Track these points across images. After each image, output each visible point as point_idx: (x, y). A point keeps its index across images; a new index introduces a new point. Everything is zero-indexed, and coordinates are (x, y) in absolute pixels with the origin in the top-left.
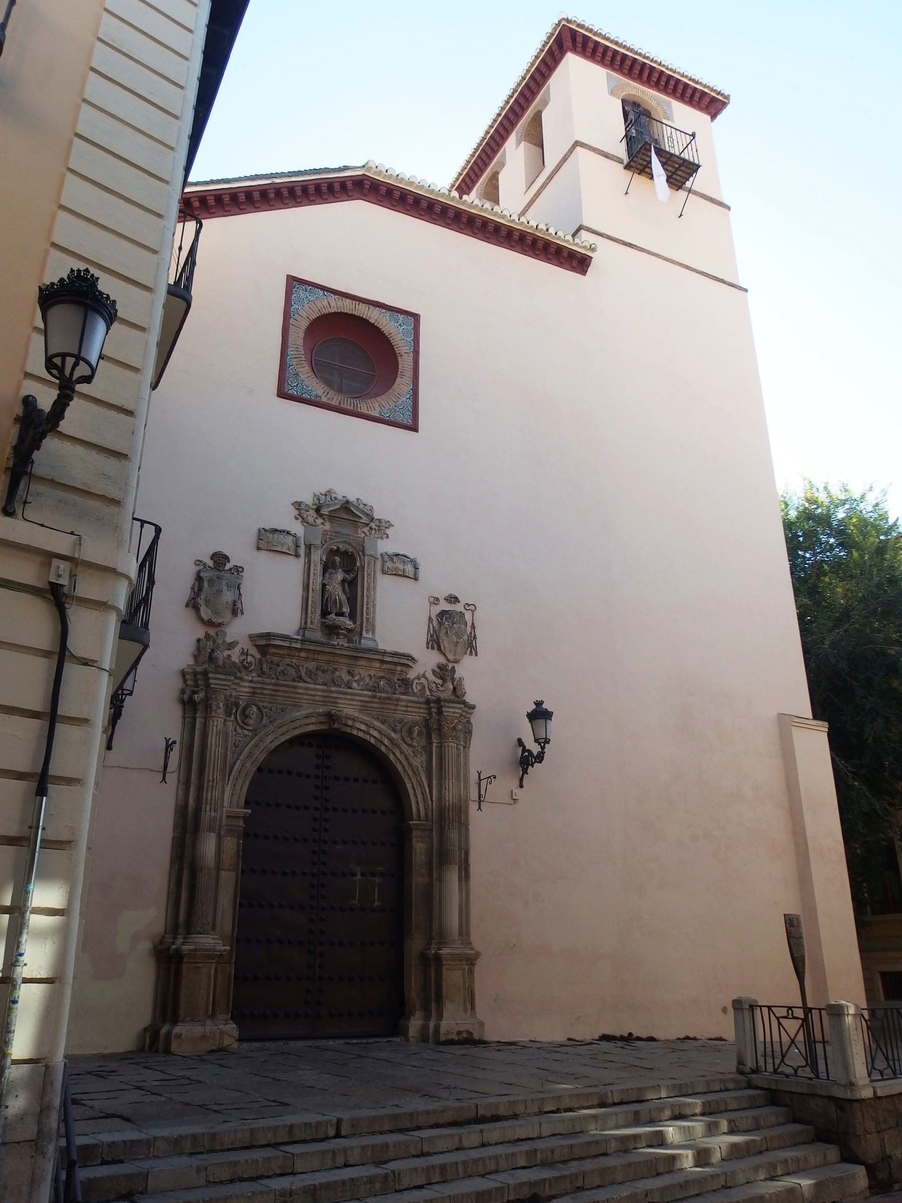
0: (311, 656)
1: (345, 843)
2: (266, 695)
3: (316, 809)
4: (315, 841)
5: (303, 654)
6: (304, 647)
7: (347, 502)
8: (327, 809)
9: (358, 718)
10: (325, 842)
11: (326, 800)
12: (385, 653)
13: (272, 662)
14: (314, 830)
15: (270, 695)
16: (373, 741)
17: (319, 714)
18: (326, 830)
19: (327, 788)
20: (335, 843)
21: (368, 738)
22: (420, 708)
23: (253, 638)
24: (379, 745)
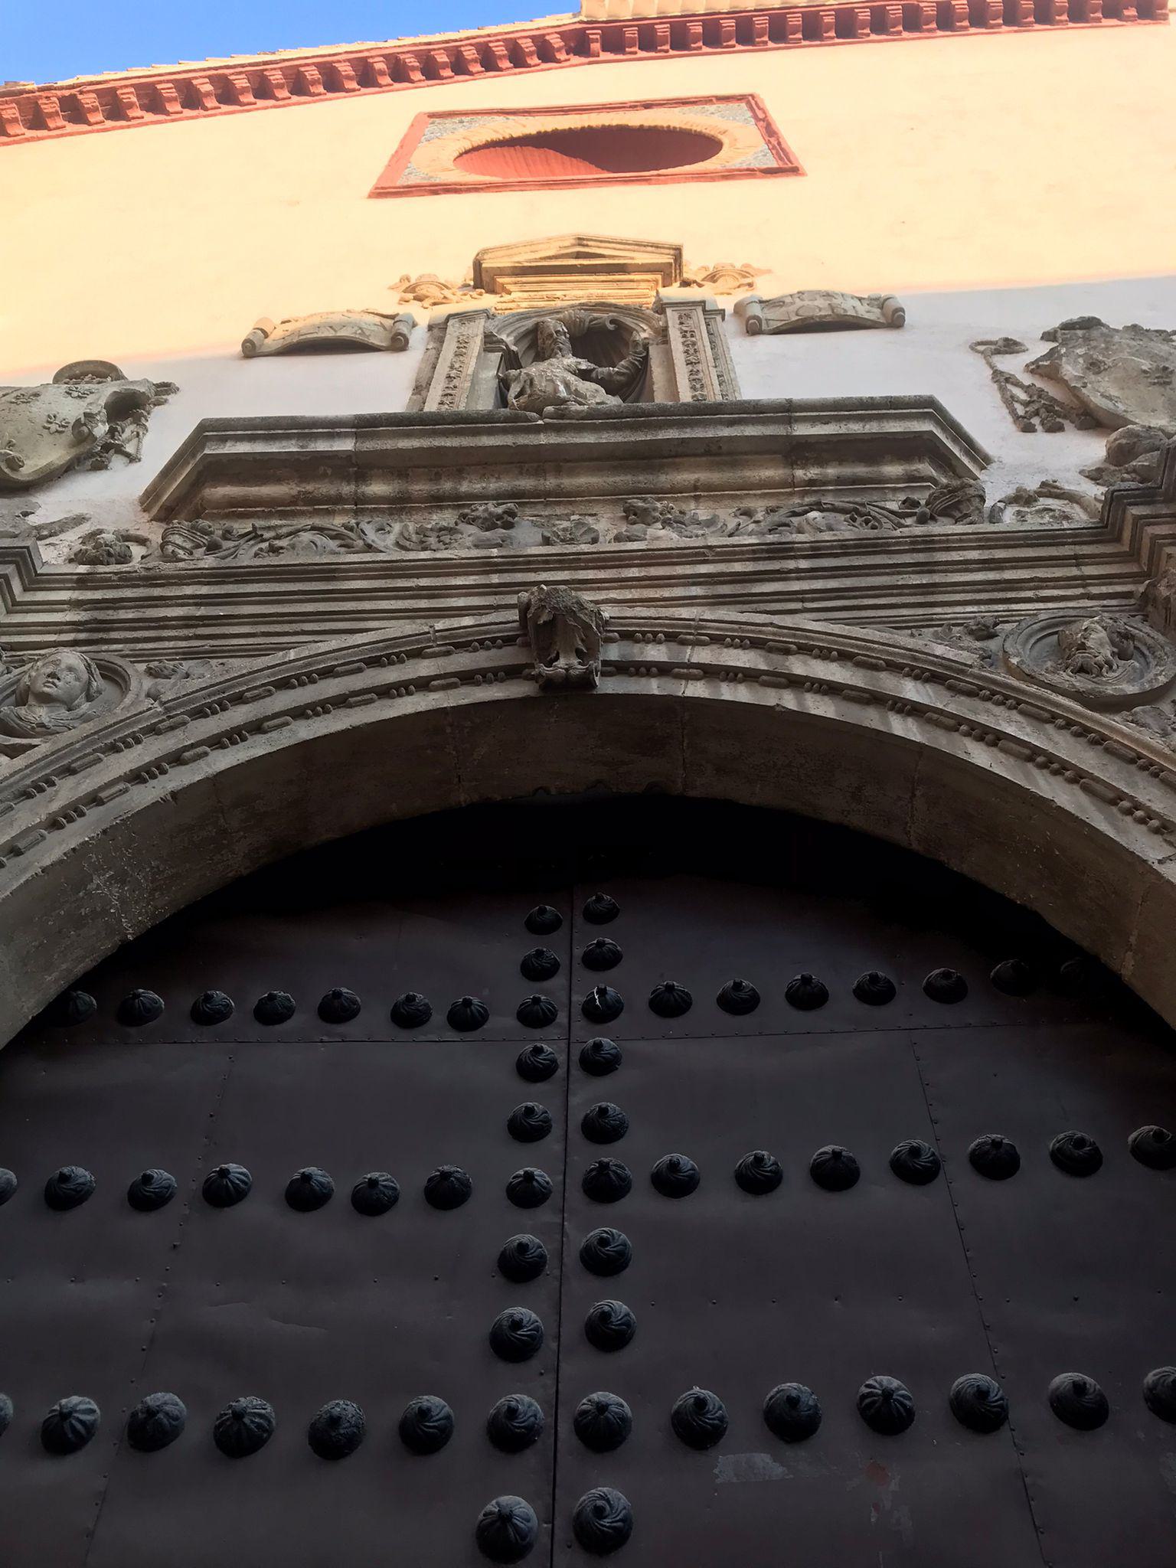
0: (420, 488)
1: (790, 1425)
2: (162, 623)
3: (526, 1195)
4: (509, 1436)
5: (377, 488)
6: (369, 445)
7: (581, 241)
8: (604, 1187)
9: (699, 624)
10: (601, 1434)
11: (601, 1129)
12: (788, 411)
13: (227, 535)
14: (512, 1346)
15: (188, 622)
16: (821, 707)
17: (459, 643)
18: (607, 1336)
19: (598, 1064)
20: (696, 1432)
21: (789, 700)
22: (1078, 560)
23: (149, 499)
24: (871, 718)
